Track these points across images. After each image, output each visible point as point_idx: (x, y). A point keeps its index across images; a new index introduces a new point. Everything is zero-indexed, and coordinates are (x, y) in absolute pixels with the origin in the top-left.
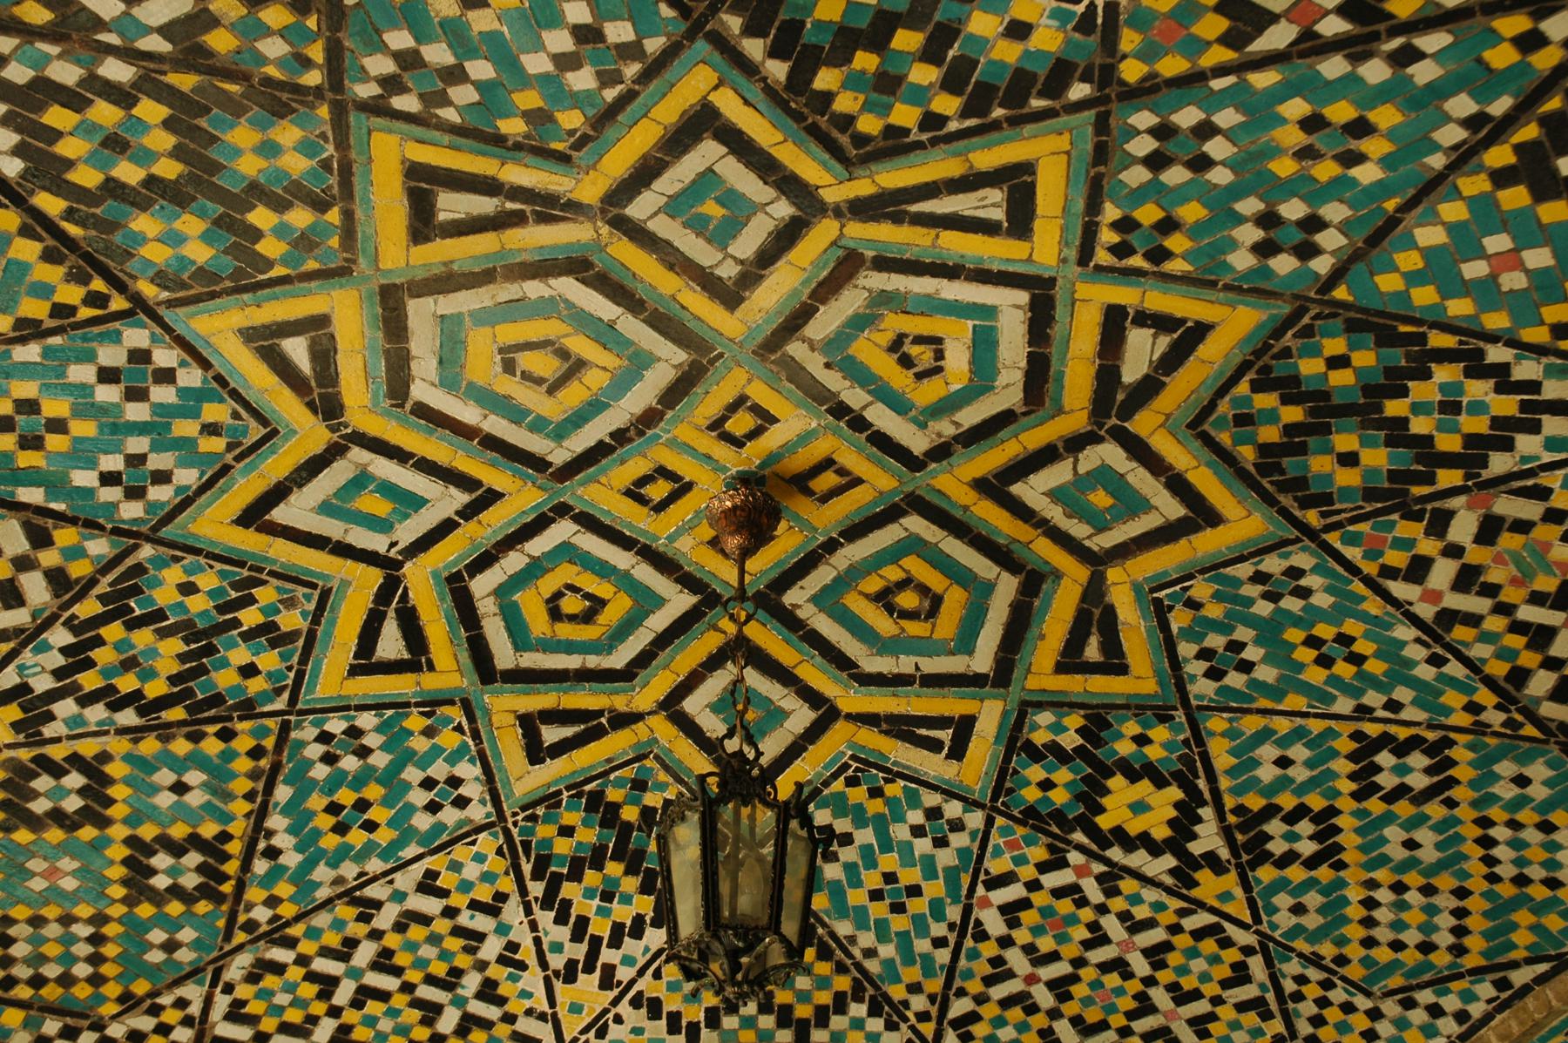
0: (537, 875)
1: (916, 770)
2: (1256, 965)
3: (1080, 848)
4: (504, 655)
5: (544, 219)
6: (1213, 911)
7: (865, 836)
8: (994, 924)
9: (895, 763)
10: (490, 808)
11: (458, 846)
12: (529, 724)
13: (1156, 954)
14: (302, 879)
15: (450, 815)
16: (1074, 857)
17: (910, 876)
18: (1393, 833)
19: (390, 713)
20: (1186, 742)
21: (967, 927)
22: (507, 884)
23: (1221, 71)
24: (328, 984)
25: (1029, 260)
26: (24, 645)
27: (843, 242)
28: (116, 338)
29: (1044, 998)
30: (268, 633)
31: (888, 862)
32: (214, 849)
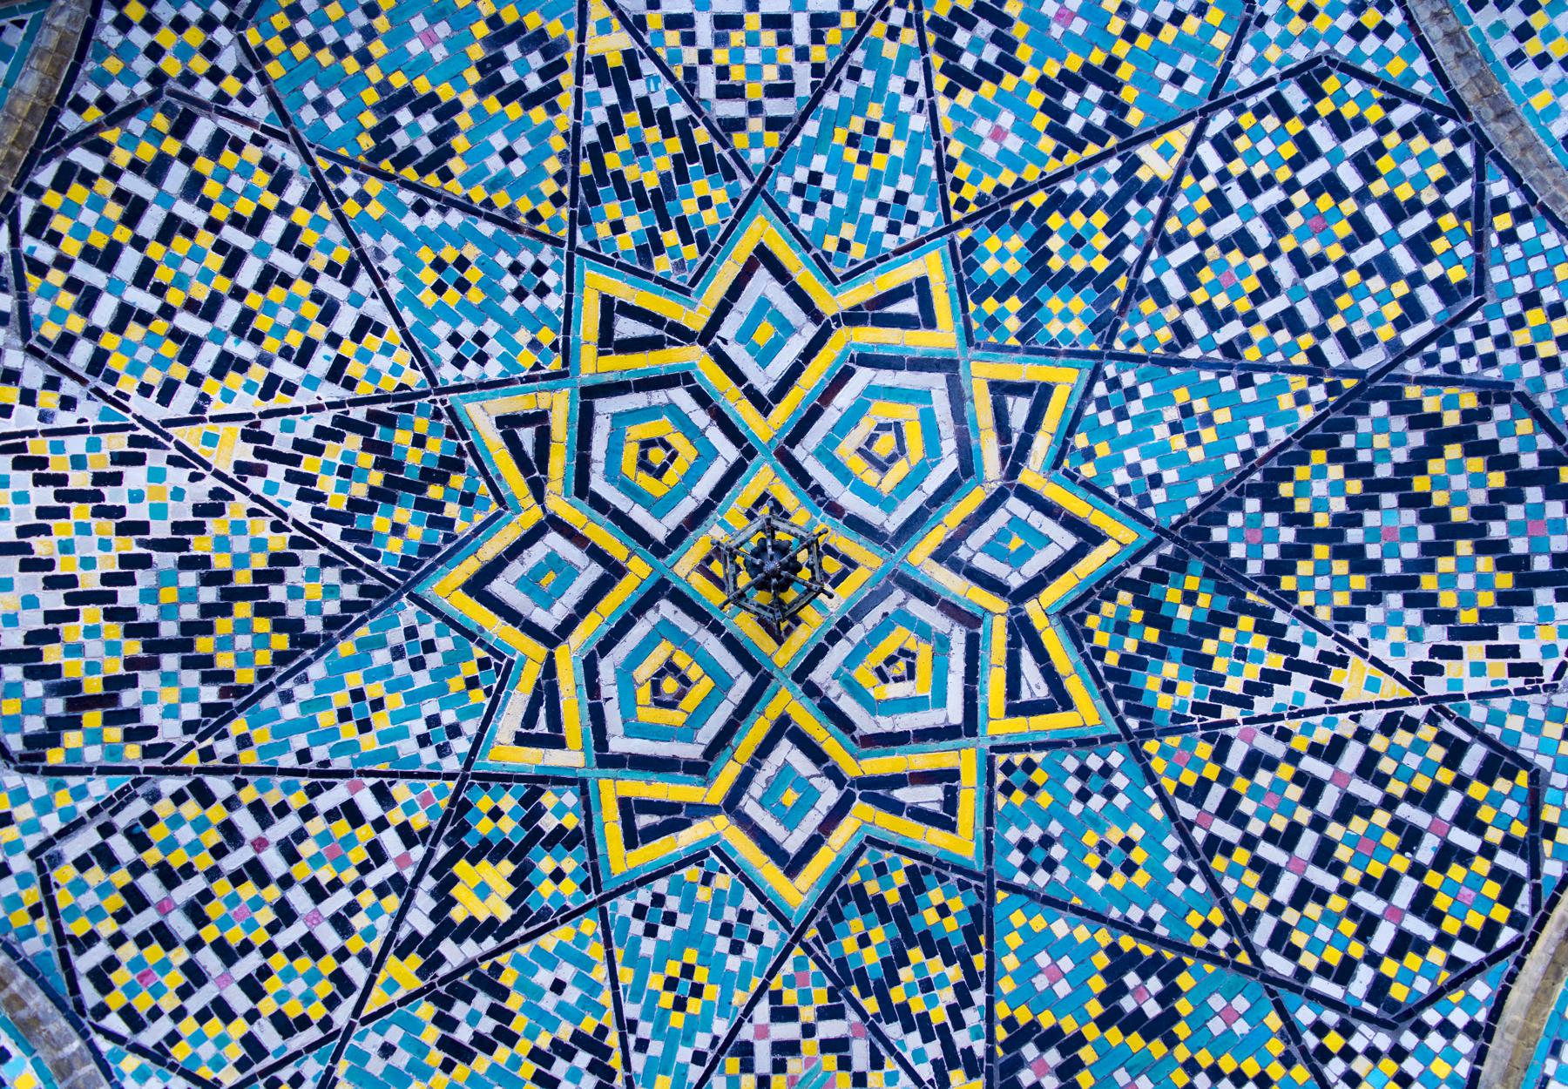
0: (372, 415)
1: (502, 711)
3: (430, 855)
5: (1004, 455)
6: (371, 981)
9: (508, 695)
10: (452, 383)
11: (410, 354)
12: (539, 419)
16: (418, 852)
19: (561, 319)
20: (565, 908)
21: (325, 776)
22: (364, 389)
23: (1159, 790)
25: (989, 719)
26: (678, 86)
27: (988, 616)
28: (930, 207)
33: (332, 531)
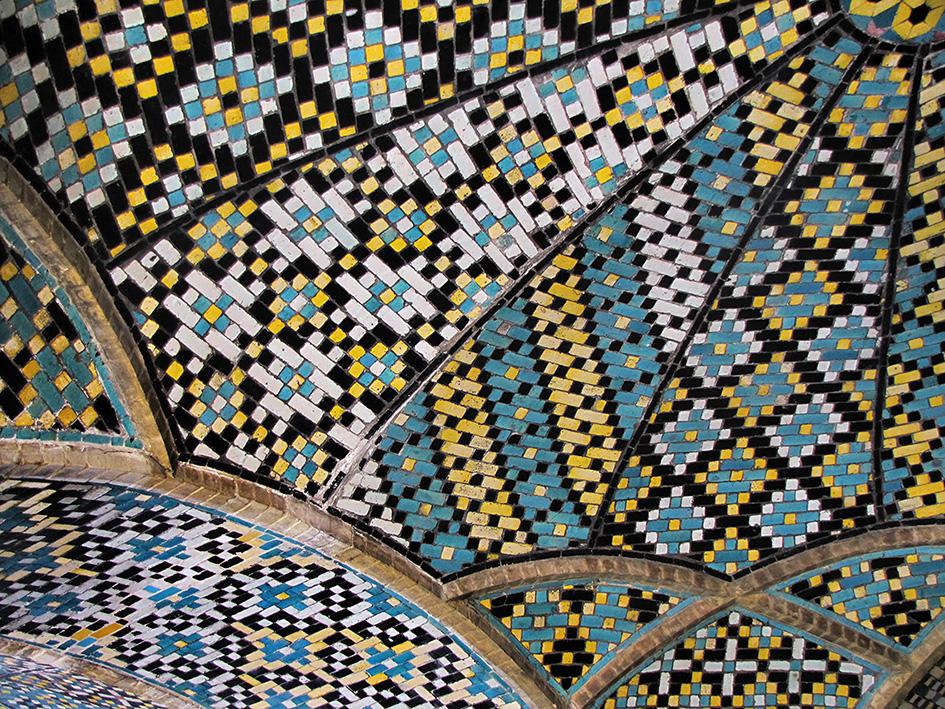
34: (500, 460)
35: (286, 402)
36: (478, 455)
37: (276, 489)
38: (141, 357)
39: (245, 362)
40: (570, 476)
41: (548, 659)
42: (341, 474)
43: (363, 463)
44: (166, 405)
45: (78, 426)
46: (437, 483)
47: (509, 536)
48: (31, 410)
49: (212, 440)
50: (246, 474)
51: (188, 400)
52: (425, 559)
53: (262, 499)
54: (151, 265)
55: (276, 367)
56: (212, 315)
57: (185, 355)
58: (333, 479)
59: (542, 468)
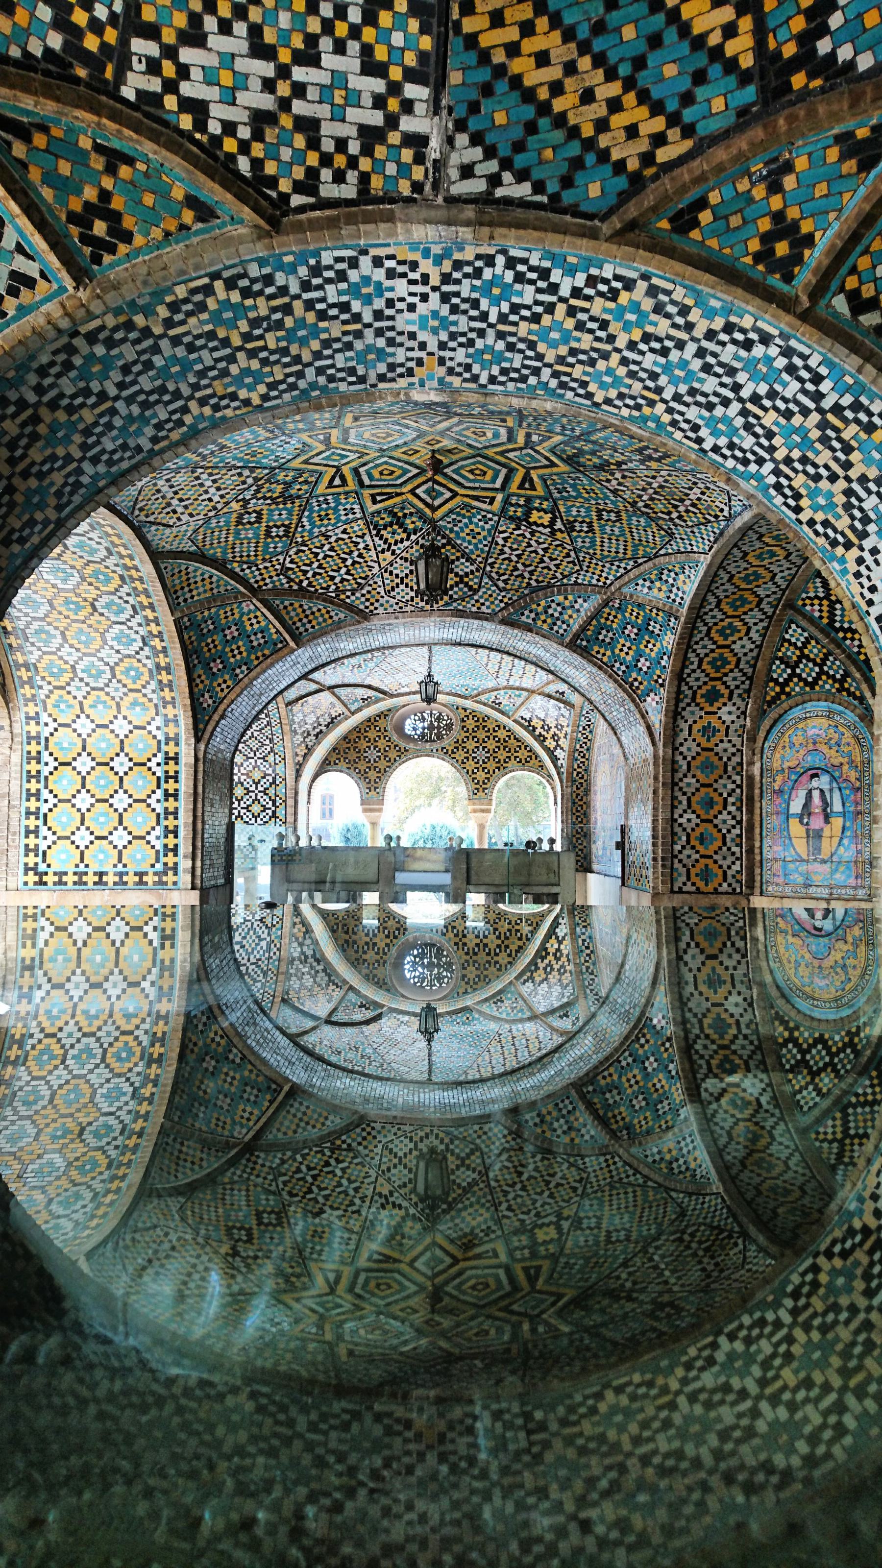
2: (572, 554)
4: (367, 481)
7: (466, 521)
8: (501, 542)
12: (373, 497)
13: (545, 550)
14: (310, 532)
15: (351, 516)
17: (477, 530)
18: (608, 529)
21: (494, 542)
24: (316, 555)
29: (514, 558)
30: (306, 482)
31: (472, 527)
32: (288, 527)
33: (413, 537)
34: (599, 60)
35: (343, 120)
36: (570, 68)
37: (383, 203)
38: (195, 149)
39: (285, 104)
40: (696, 31)
41: (758, 258)
42: (435, 161)
43: (450, 141)
44: (242, 178)
45: (183, 227)
46: (544, 123)
47: (659, 140)
48: (139, 232)
49: (299, 187)
50: (348, 203)
51: (257, 164)
52: (571, 206)
53: (369, 219)
54: (143, 67)
55: (312, 93)
56: (226, 79)
57: (229, 128)
58: (431, 171)
59: (655, 41)
